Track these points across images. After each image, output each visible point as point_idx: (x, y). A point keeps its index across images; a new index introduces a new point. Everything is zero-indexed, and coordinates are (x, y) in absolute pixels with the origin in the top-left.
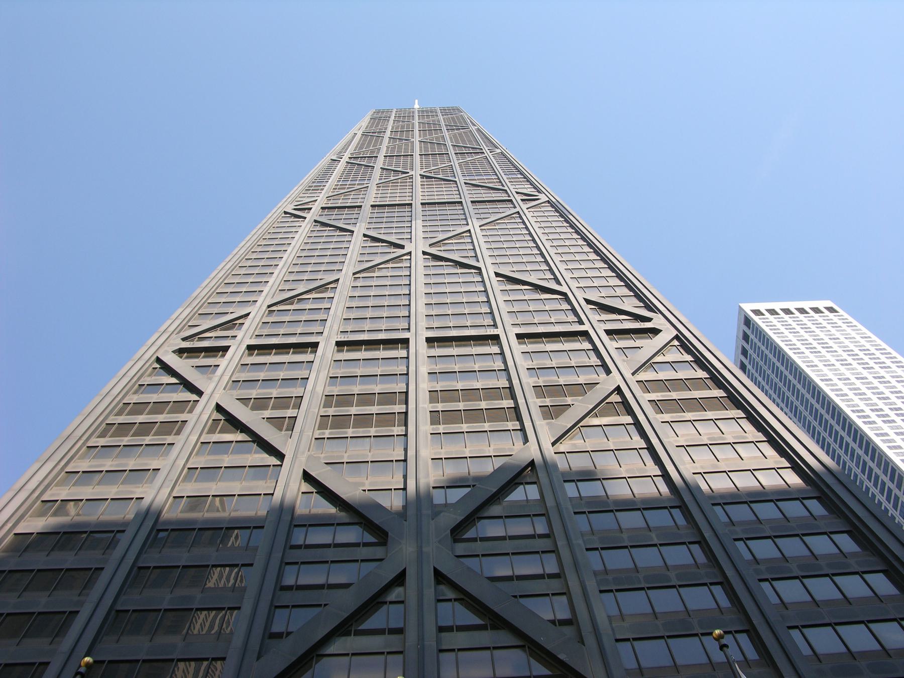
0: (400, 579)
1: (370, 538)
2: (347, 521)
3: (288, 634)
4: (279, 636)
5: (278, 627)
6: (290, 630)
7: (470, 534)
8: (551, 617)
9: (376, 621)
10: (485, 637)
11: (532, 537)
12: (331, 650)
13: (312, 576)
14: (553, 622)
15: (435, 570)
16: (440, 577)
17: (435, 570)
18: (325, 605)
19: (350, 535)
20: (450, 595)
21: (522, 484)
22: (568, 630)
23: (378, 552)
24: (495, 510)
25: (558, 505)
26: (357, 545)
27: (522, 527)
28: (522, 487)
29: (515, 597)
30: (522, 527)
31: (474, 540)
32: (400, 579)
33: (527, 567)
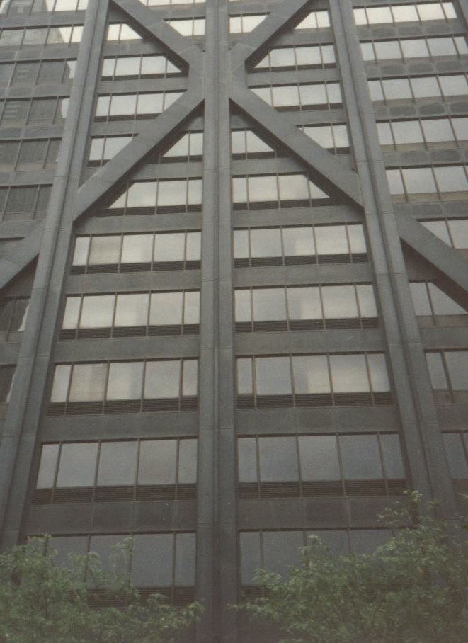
0: (199, 111)
1: (173, 69)
2: (152, 52)
3: (105, 162)
4: (96, 164)
5: (95, 155)
6: (105, 159)
7: (263, 64)
8: (330, 145)
9: (179, 149)
10: (273, 164)
11: (318, 67)
12: (139, 177)
13: (123, 106)
14: (331, 151)
15: (230, 99)
16: (235, 109)
17: (230, 99)
18: (135, 135)
19: (157, 65)
20: (243, 125)
21: (313, 11)
22: (344, 158)
23: (179, 83)
24: (288, 39)
25: (345, 35)
26: (160, 76)
27: (308, 56)
28: (312, 14)
29: (299, 126)
30: (308, 56)
31: (266, 70)
32: (199, 111)
33: (313, 95)
